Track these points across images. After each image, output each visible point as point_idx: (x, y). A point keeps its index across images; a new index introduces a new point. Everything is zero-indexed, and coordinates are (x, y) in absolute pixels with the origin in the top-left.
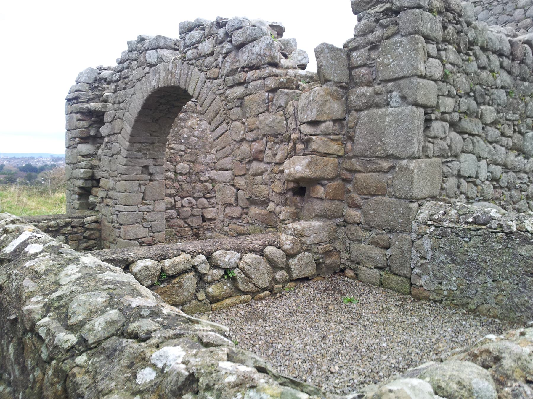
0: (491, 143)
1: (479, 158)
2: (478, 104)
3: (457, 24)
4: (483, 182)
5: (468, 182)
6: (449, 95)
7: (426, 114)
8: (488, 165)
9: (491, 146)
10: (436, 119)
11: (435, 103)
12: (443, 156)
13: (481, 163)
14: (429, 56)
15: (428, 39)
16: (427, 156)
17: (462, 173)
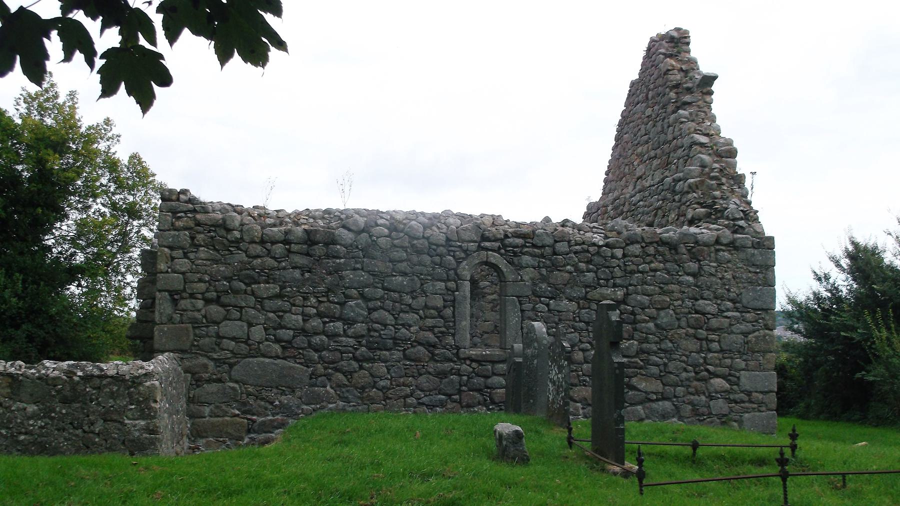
0: (274, 312)
1: (250, 325)
2: (247, 285)
3: (209, 232)
4: (259, 343)
5: (237, 342)
6: (201, 280)
7: (171, 295)
8: (266, 329)
9: (271, 315)
10: (182, 298)
11: (182, 287)
12: (197, 323)
13: (253, 329)
14: (173, 259)
15: (171, 248)
16: (173, 323)
17: (221, 335)
